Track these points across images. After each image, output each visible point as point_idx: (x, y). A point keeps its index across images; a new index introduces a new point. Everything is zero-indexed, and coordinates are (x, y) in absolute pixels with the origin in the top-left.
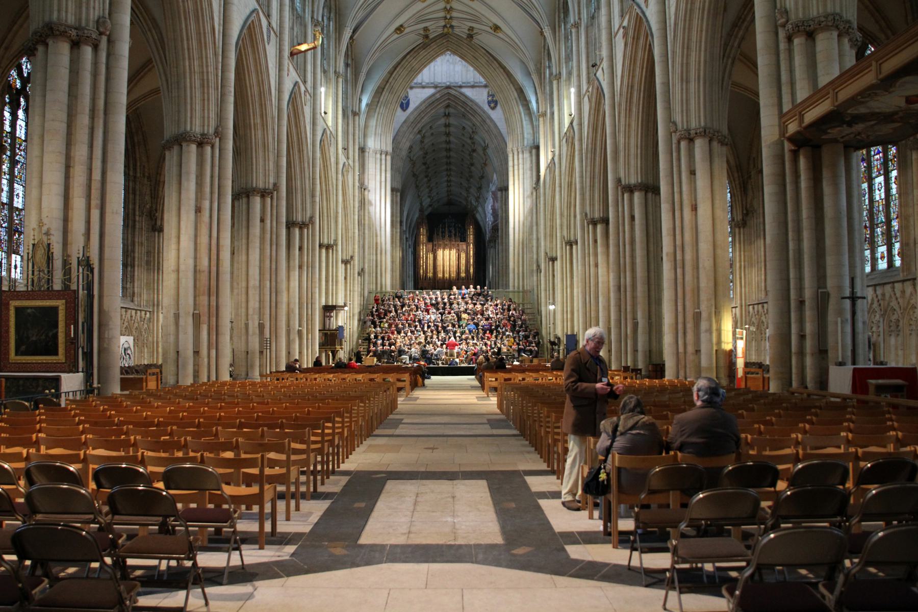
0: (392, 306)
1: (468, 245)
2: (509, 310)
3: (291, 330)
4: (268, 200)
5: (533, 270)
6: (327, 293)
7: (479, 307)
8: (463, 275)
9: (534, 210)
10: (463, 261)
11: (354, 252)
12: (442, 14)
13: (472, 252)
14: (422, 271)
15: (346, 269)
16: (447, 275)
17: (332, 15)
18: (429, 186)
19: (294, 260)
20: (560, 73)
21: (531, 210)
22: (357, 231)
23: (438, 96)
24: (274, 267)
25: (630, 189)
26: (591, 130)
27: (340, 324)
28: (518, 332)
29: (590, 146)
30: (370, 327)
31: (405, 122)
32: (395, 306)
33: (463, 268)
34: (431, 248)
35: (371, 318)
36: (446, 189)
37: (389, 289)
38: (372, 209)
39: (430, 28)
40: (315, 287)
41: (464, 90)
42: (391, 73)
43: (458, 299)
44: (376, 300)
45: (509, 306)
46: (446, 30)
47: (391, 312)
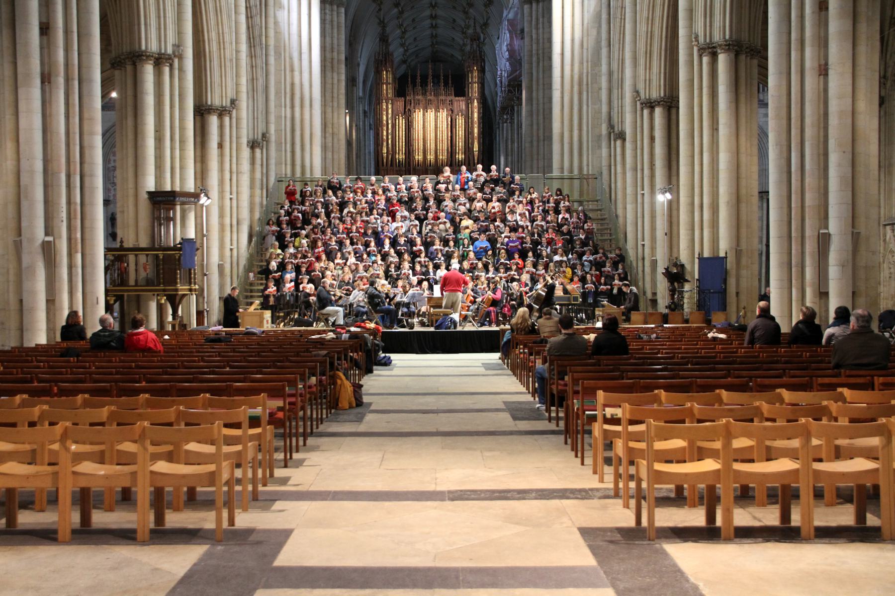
0: (319, 205)
1: (469, 102)
2: (557, 212)
3: (25, 244)
5: (600, 136)
6: (159, 167)
7: (496, 205)
9: (604, 16)
10: (460, 132)
11: (237, 92)
13: (476, 115)
14: (385, 150)
15: (221, 127)
16: (431, 157)
18: (401, 26)
19: (27, 56)
21: (598, 16)
22: (244, 47)
27: (191, 234)
28: (580, 255)
30: (273, 246)
32: (326, 205)
33: (460, 144)
34: (401, 109)
35: (274, 228)
36: (428, 32)
37: (318, 174)
38: (282, 15)
40: (92, 134)
43: (454, 190)
44: (290, 194)
45: (557, 203)
47: (317, 216)
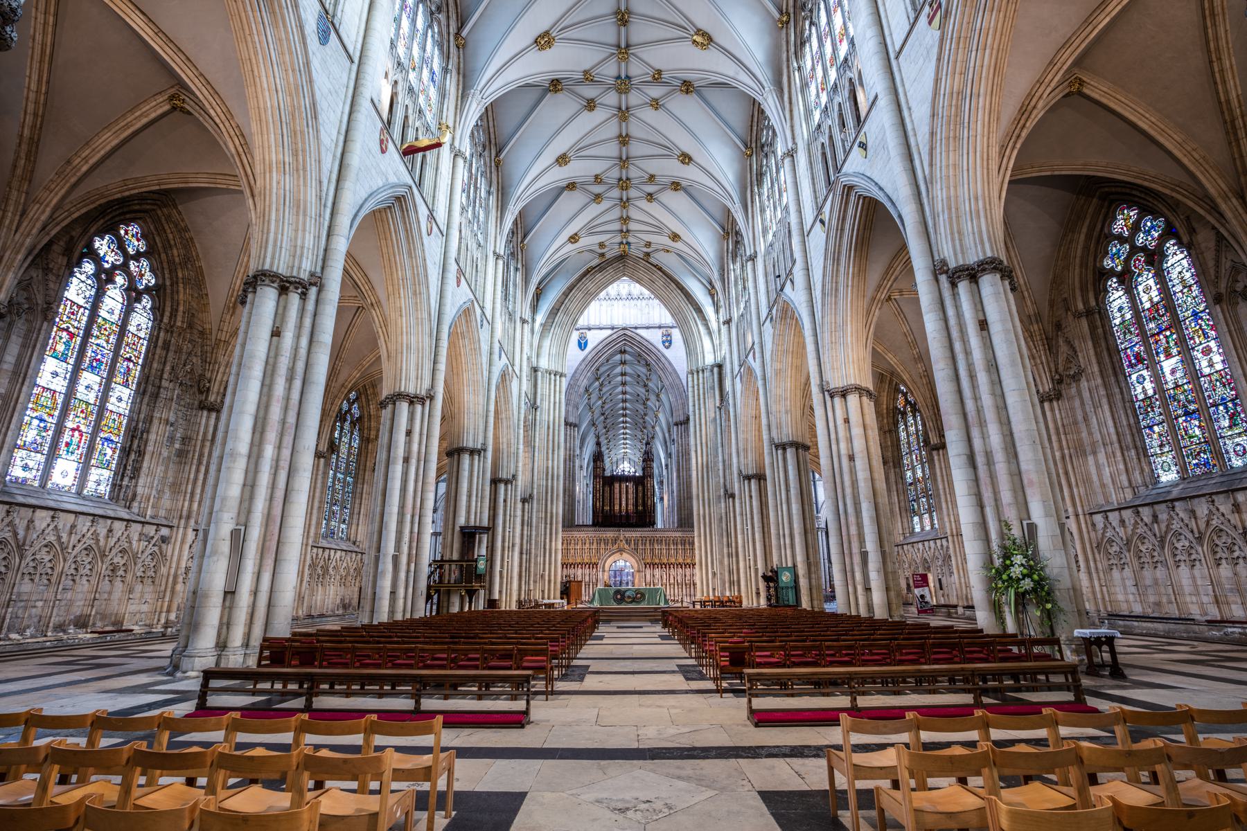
4: (294, 299)
8: (640, 508)
10: (640, 495)
12: (617, 226)
15: (506, 490)
17: (493, 189)
20: (756, 252)
23: (615, 336)
24: (291, 419)
25: (972, 274)
26: (829, 262)
29: (828, 286)
31: (583, 360)
39: (606, 244)
41: (638, 331)
42: (566, 294)
46: (622, 246)
